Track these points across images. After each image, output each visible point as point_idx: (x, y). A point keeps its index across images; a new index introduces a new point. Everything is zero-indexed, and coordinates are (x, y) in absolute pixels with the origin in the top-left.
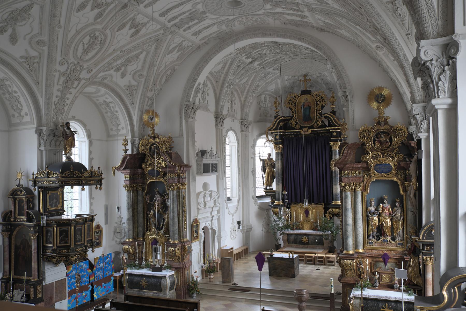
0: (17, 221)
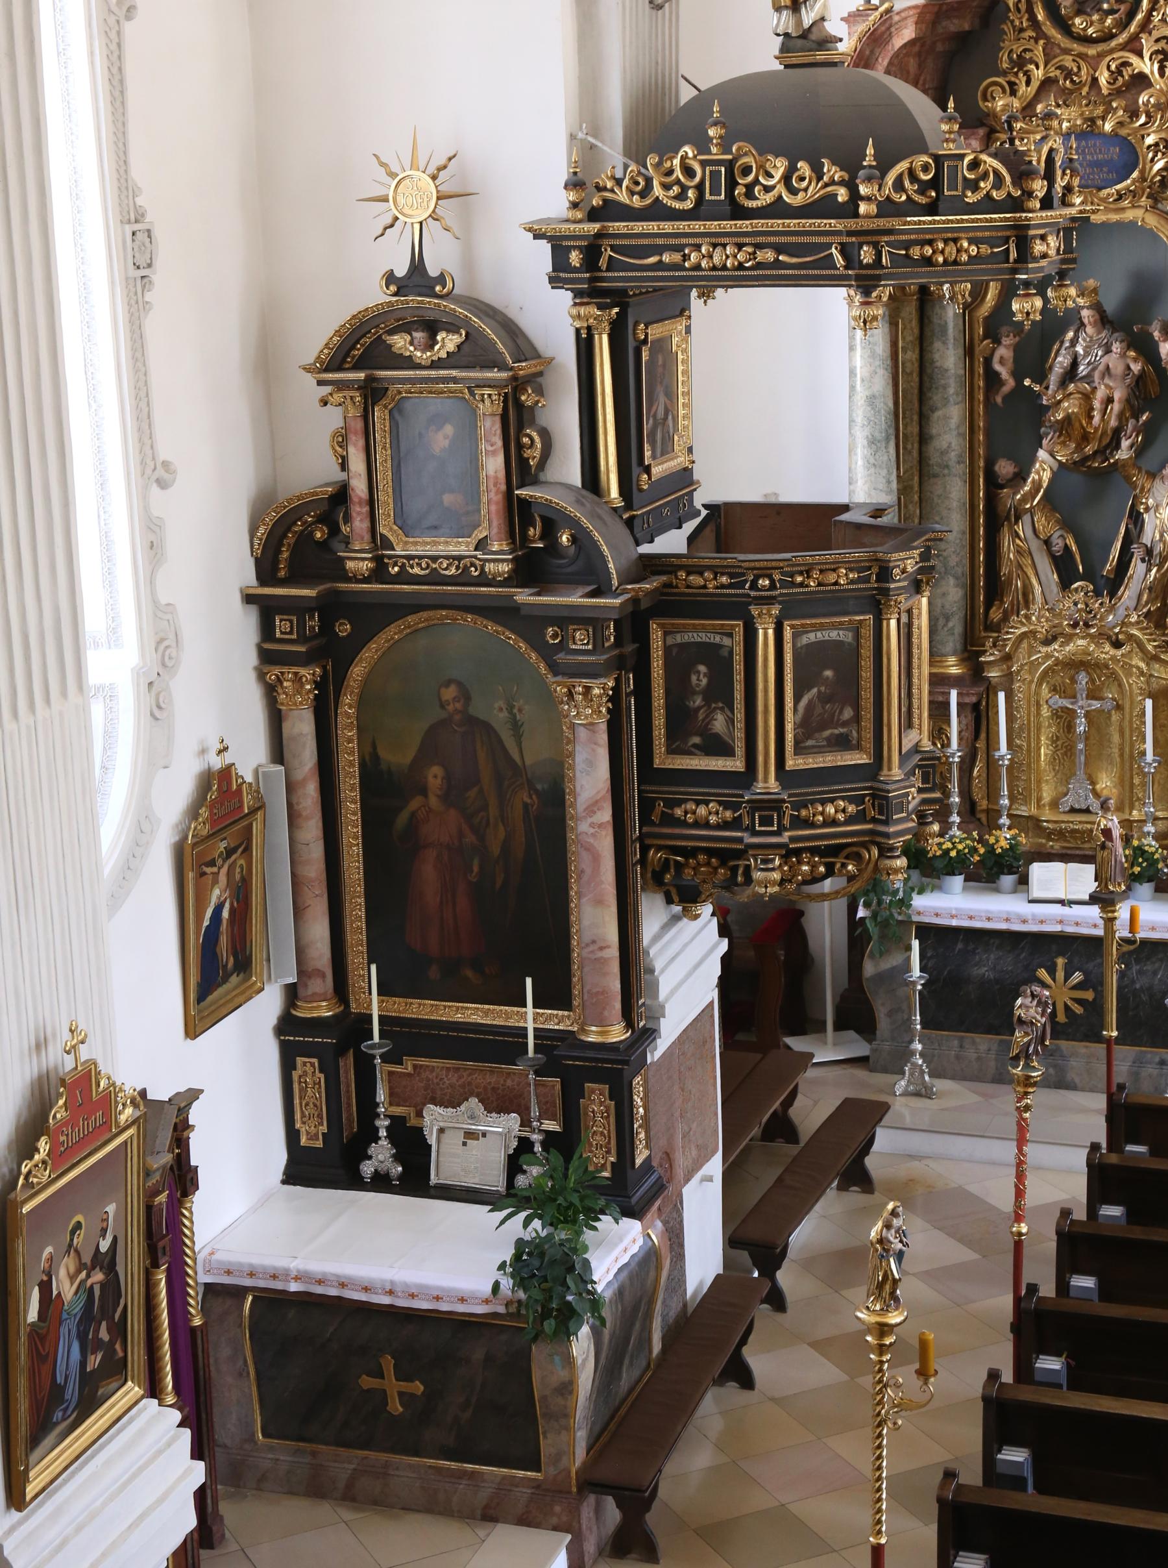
0: (403, 577)
